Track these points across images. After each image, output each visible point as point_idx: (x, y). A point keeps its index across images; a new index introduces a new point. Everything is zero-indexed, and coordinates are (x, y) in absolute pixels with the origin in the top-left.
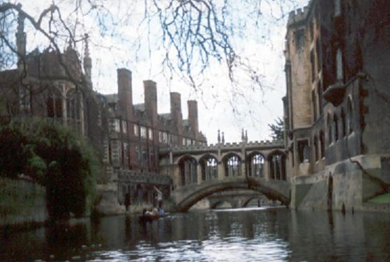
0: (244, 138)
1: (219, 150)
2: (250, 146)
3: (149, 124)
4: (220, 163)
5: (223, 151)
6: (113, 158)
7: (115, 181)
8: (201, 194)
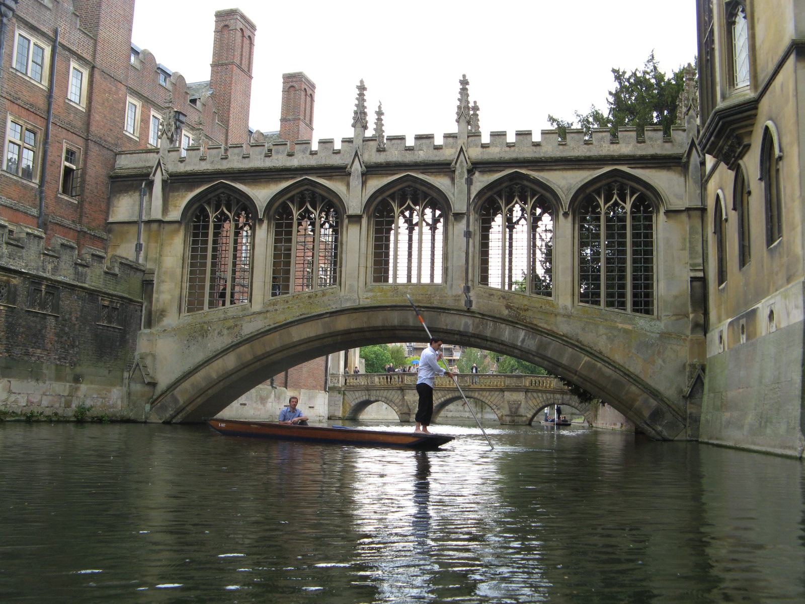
0: (467, 114)
1: (357, 168)
2: (495, 153)
4: (355, 219)
5: (371, 170)
8: (260, 348)
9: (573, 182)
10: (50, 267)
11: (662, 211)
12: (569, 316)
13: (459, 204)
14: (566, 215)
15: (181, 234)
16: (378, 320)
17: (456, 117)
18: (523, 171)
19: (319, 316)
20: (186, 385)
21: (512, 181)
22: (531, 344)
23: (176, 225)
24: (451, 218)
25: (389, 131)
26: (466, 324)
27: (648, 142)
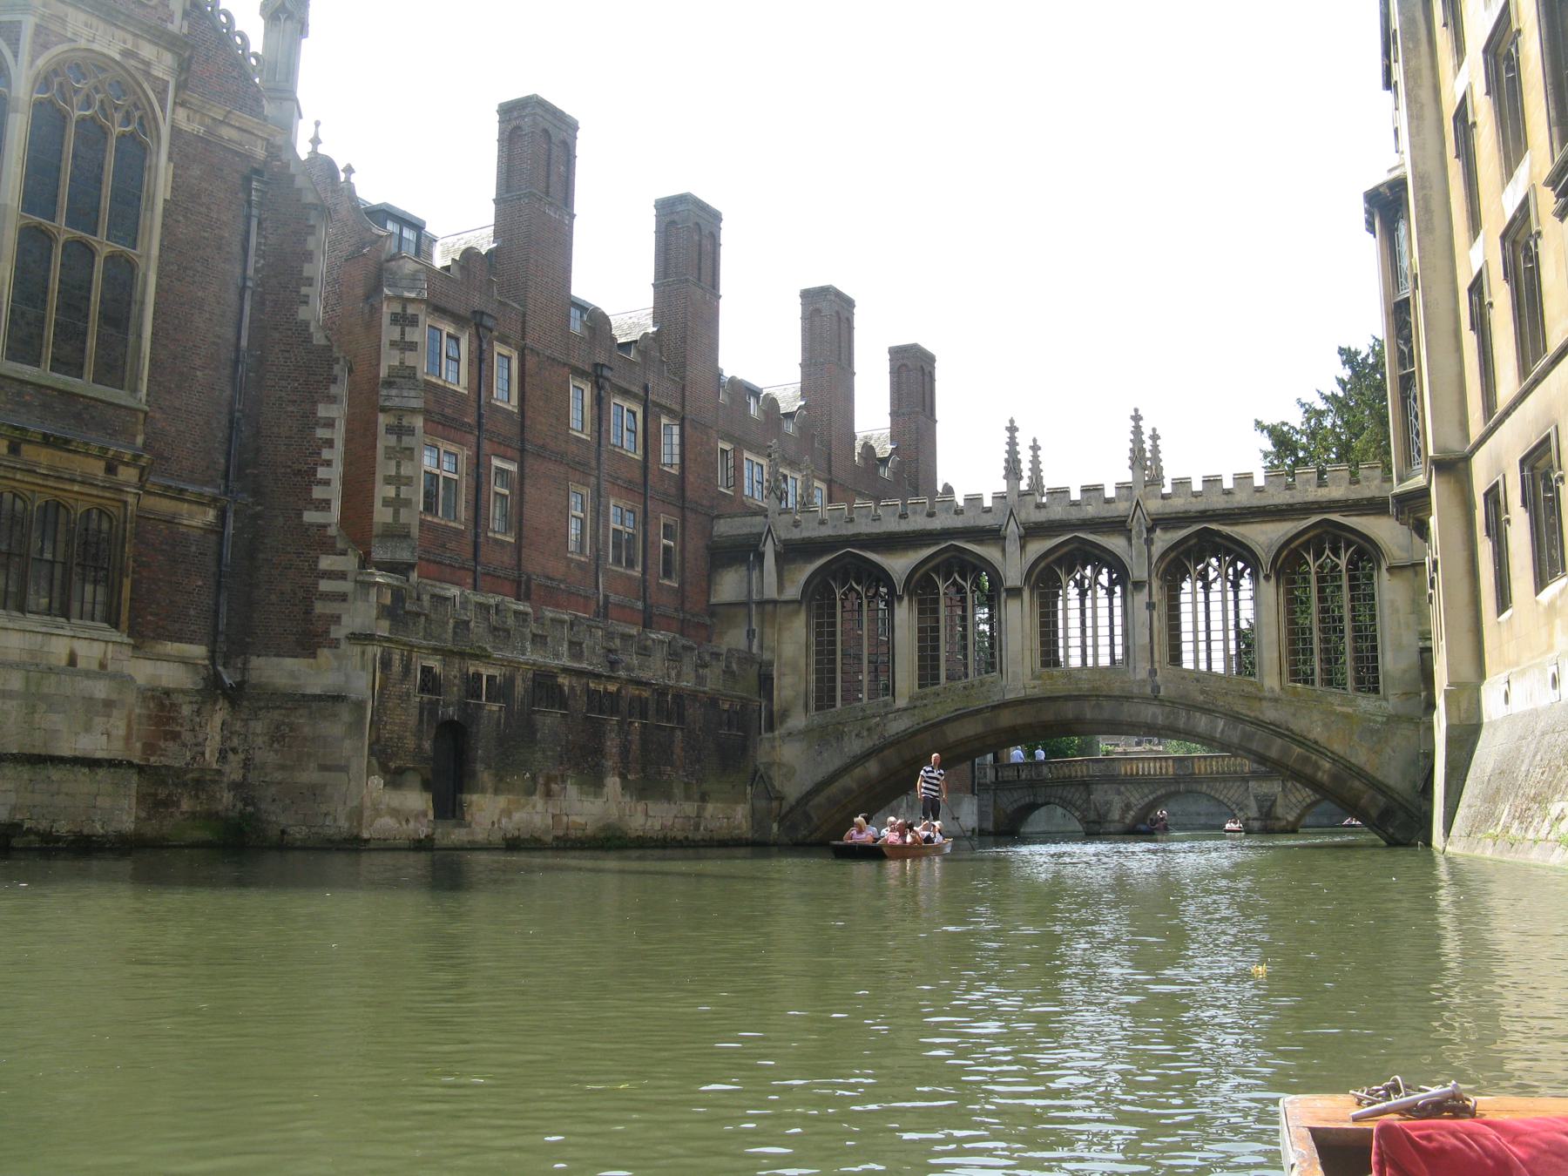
0: (1144, 458)
1: (1013, 530)
2: (1179, 504)
3: (662, 391)
4: (1015, 592)
5: (1033, 531)
6: (382, 515)
7: (356, 638)
9: (1274, 536)
10: (673, 673)
11: (1384, 567)
12: (1276, 700)
13: (1138, 571)
14: (1267, 578)
15: (803, 617)
16: (1049, 714)
17: (1129, 463)
18: (1214, 526)
19: (979, 711)
20: (820, 799)
21: (1201, 536)
22: (1235, 736)
23: (796, 606)
24: (1130, 586)
25: (1050, 482)
26: (1154, 715)
27: (1364, 483)
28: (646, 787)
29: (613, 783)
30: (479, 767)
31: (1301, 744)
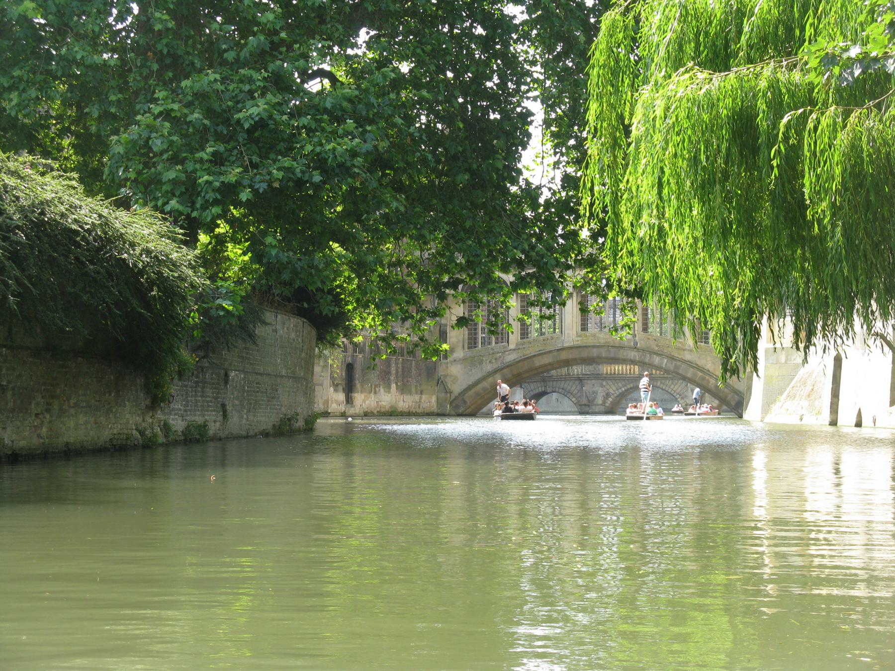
19: (551, 352)
20: (471, 393)
22: (671, 367)
26: (635, 356)
28: (404, 389)
29: (394, 386)
30: (357, 382)
31: (701, 371)
